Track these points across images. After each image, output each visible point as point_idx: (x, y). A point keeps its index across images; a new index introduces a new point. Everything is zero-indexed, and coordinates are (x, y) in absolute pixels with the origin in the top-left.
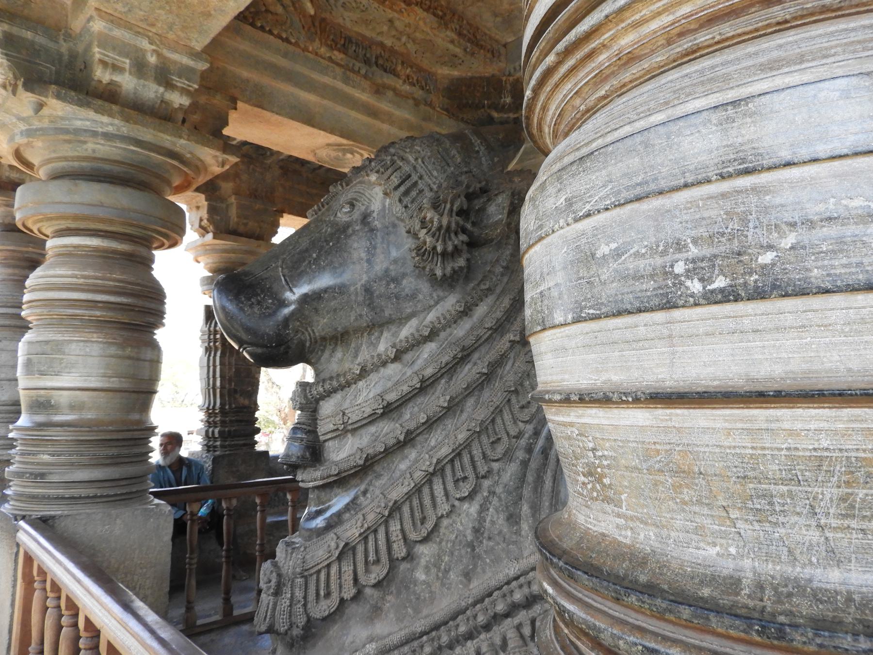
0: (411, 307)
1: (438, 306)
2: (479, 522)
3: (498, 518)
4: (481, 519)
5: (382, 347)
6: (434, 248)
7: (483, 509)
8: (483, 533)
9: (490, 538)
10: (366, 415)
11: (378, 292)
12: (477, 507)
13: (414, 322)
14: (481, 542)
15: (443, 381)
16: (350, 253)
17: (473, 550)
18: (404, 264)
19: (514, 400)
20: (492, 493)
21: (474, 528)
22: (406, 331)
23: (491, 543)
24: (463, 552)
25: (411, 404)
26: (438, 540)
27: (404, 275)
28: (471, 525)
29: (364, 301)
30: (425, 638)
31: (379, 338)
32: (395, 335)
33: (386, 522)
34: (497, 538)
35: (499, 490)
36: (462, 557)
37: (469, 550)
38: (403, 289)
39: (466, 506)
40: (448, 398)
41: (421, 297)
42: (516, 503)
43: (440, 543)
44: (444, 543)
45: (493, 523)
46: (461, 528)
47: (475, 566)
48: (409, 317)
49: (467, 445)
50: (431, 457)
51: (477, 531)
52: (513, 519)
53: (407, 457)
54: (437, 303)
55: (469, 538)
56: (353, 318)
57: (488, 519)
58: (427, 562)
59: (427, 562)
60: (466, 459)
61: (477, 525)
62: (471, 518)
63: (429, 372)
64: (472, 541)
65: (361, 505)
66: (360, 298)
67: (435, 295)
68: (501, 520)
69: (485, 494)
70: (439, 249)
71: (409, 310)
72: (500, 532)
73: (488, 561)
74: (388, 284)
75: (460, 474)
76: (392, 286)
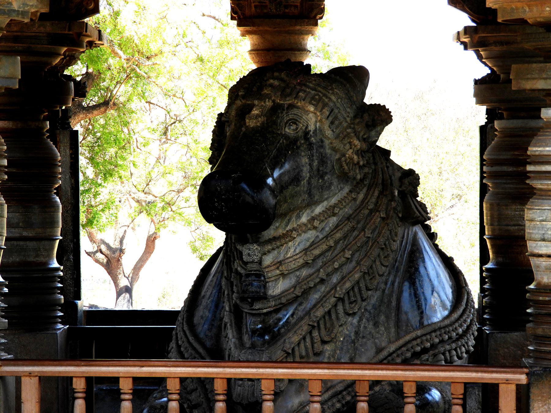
0: (327, 194)
1: (339, 194)
2: (359, 329)
3: (369, 324)
4: (359, 326)
5: (304, 219)
6: (358, 163)
7: (361, 320)
8: (359, 335)
9: (363, 337)
10: (299, 264)
11: (313, 185)
12: (358, 318)
13: (325, 203)
14: (358, 340)
15: (341, 242)
16: (300, 159)
17: (355, 345)
18: (326, 166)
19: (381, 254)
20: (366, 310)
21: (355, 331)
22: (318, 210)
23: (364, 340)
24: (349, 347)
25: (322, 257)
26: (335, 340)
27: (326, 173)
28: (354, 330)
29: (307, 190)
30: (344, 393)
31: (303, 213)
32: (312, 212)
33: (310, 333)
34: (368, 336)
35: (369, 308)
36: (349, 349)
37: (353, 345)
38: (325, 183)
39: (350, 319)
40: (351, 252)
41: (333, 188)
42: (378, 315)
43: (336, 342)
44: (337, 343)
45: (365, 327)
46: (347, 333)
47: (355, 354)
48: (322, 202)
49: (358, 282)
50: (341, 289)
51: (357, 333)
52: (376, 324)
53: (319, 291)
54: (339, 191)
55: (353, 338)
56: (300, 202)
57: (362, 326)
58: (329, 354)
59: (329, 354)
60: (356, 290)
61: (357, 329)
62: (354, 325)
63: (338, 235)
64: (354, 340)
65: (290, 322)
66: (305, 189)
67: (339, 187)
68: (370, 326)
69: (363, 311)
70: (361, 163)
71: (326, 197)
72: (370, 333)
73: (363, 350)
74: (318, 180)
75: (353, 299)
76: (320, 181)
